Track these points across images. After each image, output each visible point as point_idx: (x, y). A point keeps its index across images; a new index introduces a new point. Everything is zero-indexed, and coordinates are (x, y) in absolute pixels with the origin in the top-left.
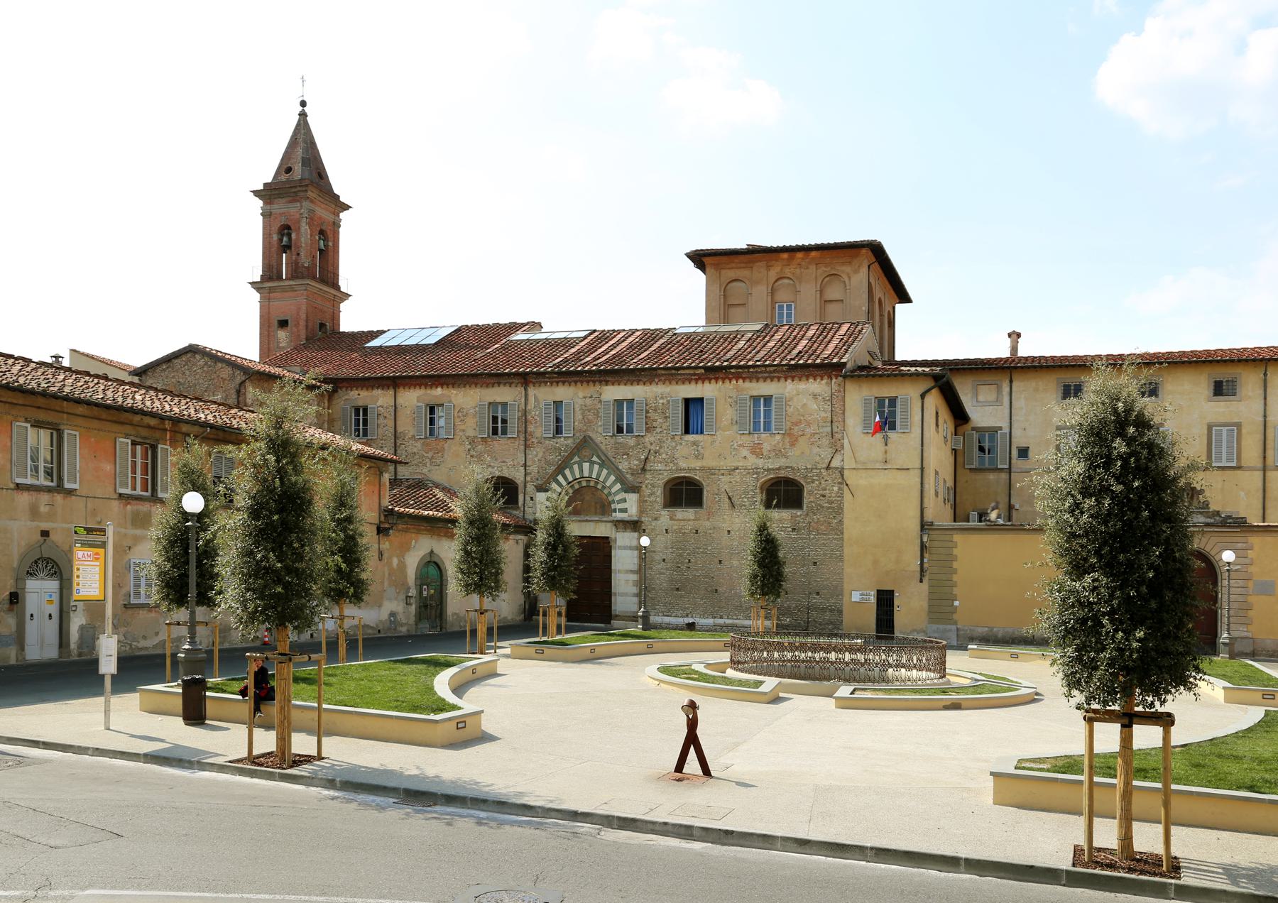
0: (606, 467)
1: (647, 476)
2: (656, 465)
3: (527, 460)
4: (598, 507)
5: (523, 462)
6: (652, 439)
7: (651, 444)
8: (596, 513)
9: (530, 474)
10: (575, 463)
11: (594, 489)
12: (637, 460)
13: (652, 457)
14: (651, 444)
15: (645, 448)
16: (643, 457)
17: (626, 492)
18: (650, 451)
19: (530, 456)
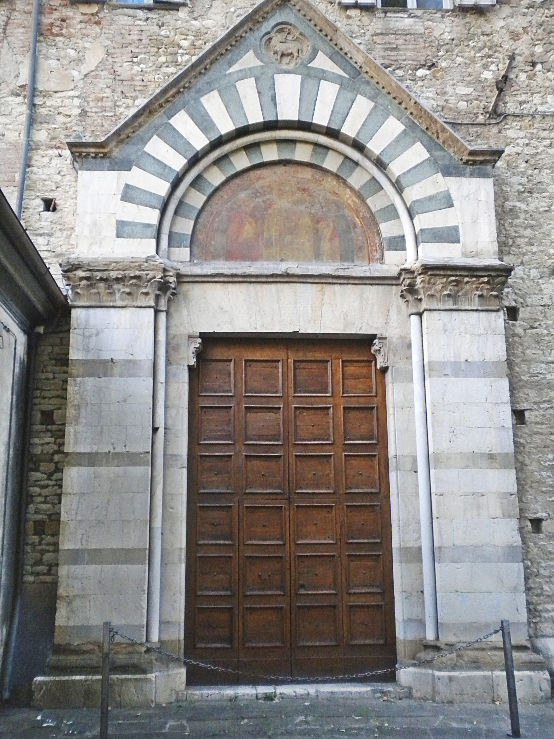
0: (368, 89)
1: (510, 133)
2: (537, 99)
3: (41, 76)
4: (327, 233)
5: (24, 78)
6: (517, 23)
7: (515, 36)
8: (317, 256)
9: (49, 119)
10: (244, 75)
11: (307, 174)
12: (468, 84)
13: (523, 77)
14: (515, 36)
15: (494, 47)
16: (488, 75)
17: (447, 172)
18: (512, 58)
19: (53, 63)
